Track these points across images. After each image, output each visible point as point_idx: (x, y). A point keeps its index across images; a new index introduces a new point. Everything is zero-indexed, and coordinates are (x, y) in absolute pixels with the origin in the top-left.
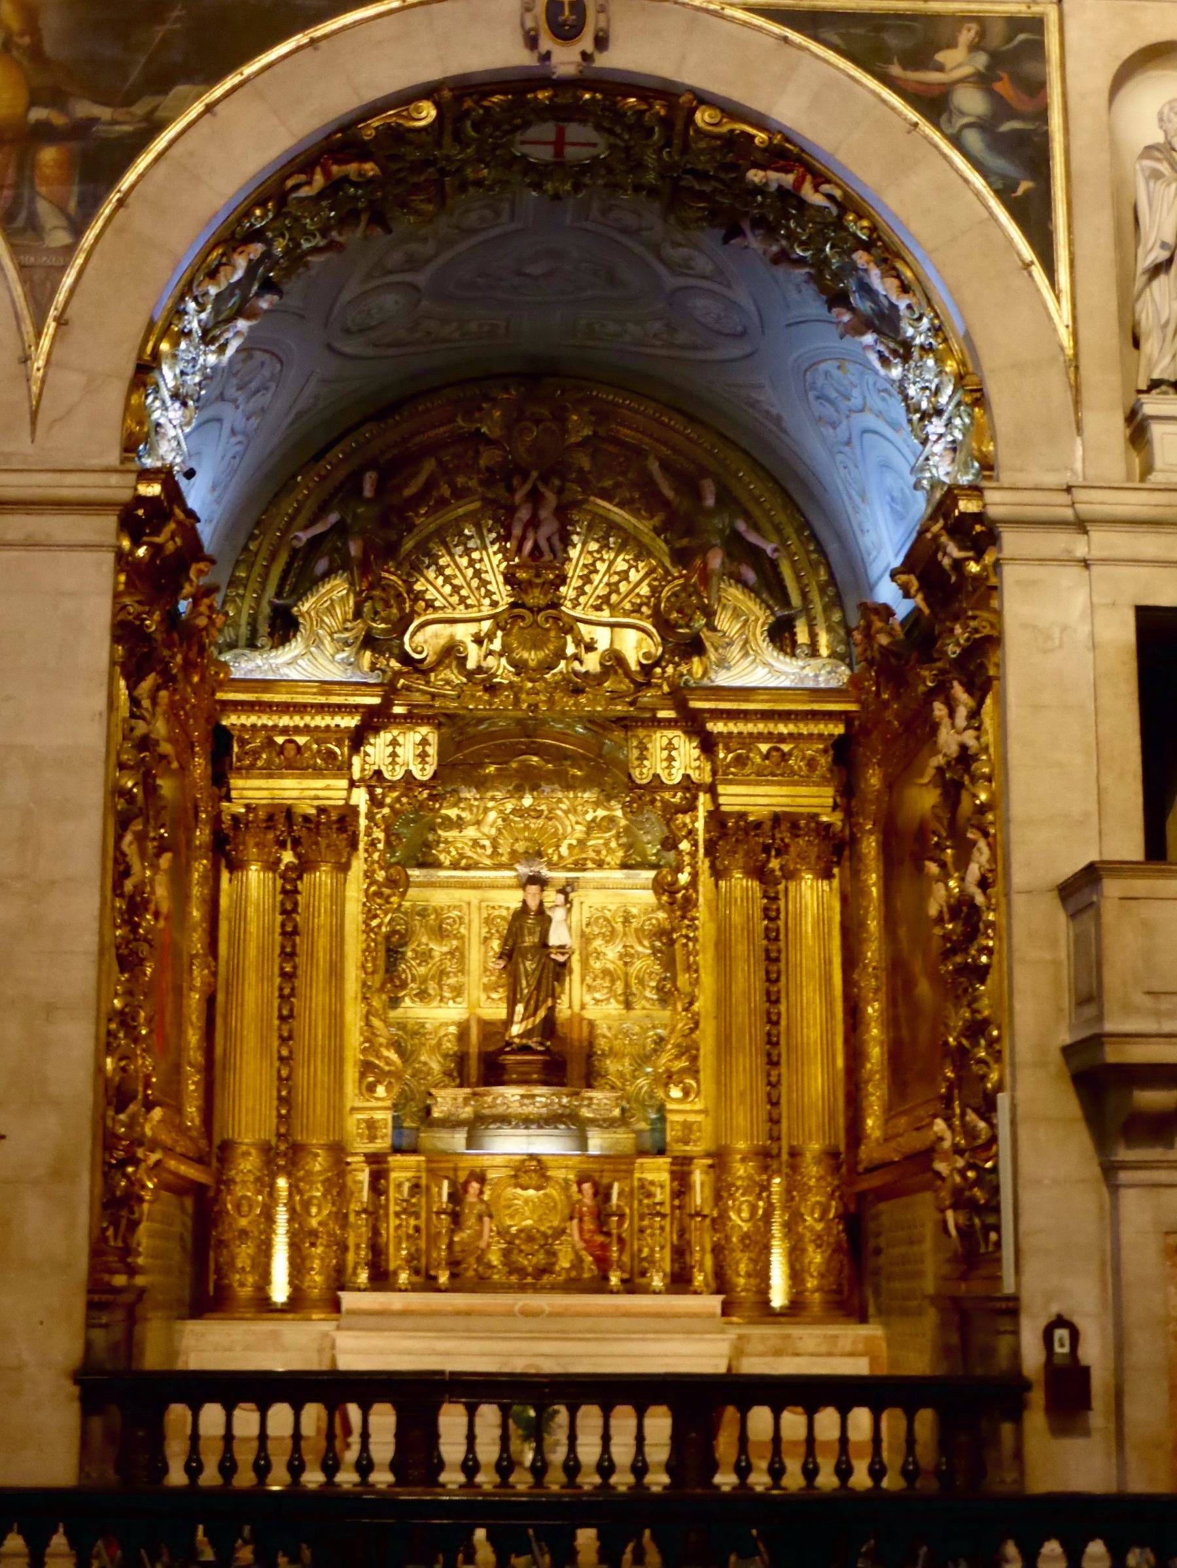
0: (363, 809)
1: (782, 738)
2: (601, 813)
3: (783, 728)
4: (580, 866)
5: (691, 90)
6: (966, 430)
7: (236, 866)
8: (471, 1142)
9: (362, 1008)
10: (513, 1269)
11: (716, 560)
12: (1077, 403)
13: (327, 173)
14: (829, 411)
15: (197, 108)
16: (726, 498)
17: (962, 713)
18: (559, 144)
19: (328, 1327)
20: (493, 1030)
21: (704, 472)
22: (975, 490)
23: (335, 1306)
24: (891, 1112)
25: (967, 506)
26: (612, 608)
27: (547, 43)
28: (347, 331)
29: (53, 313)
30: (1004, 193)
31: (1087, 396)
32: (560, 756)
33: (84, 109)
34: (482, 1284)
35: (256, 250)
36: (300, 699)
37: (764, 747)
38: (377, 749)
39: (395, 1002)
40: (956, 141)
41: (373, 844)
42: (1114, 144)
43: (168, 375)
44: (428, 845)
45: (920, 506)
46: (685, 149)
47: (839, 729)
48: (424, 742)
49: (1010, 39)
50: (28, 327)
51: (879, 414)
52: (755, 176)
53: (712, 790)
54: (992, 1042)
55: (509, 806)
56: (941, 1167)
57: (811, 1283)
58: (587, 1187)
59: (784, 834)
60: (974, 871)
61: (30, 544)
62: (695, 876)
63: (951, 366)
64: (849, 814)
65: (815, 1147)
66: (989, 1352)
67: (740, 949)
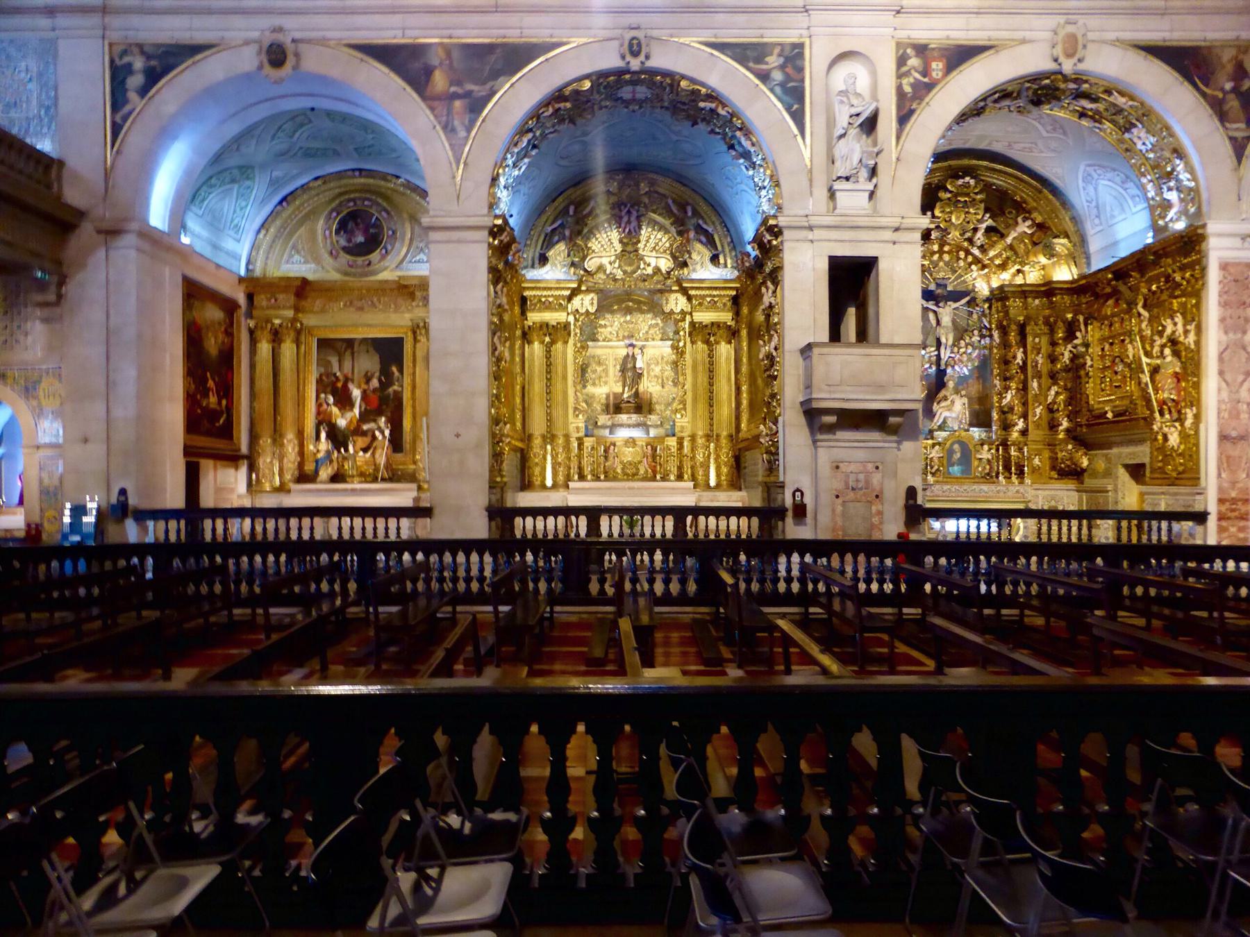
0: (572, 323)
1: (714, 296)
2: (654, 322)
3: (715, 293)
4: (646, 340)
5: (678, 74)
6: (773, 194)
7: (530, 342)
8: (611, 433)
9: (574, 389)
10: (625, 474)
11: (692, 234)
12: (811, 185)
13: (553, 107)
14: (730, 183)
15: (508, 85)
16: (696, 213)
17: (770, 291)
18: (634, 92)
19: (565, 493)
20: (617, 396)
21: (688, 204)
22: (775, 217)
23: (568, 487)
24: (749, 421)
25: (772, 222)
26: (657, 251)
27: (628, 58)
28: (562, 158)
29: (462, 161)
30: (788, 109)
31: (814, 183)
32: (639, 302)
33: (470, 87)
34: (615, 479)
35: (530, 135)
36: (549, 286)
37: (708, 299)
38: (576, 302)
39: (585, 387)
40: (772, 90)
41: (576, 334)
42: (827, 91)
43: (502, 181)
44: (594, 334)
45: (759, 219)
46: (677, 95)
47: (734, 293)
48: (592, 299)
49: (793, 50)
50: (454, 166)
51: (747, 185)
52: (702, 104)
53: (691, 314)
54: (778, 400)
55: (622, 320)
56: (762, 440)
57: (723, 478)
58: (649, 447)
59: (715, 329)
60: (773, 344)
61: (459, 241)
62: (685, 343)
63: (768, 172)
64: (737, 322)
65: (725, 433)
66: (775, 500)
67: (700, 368)
